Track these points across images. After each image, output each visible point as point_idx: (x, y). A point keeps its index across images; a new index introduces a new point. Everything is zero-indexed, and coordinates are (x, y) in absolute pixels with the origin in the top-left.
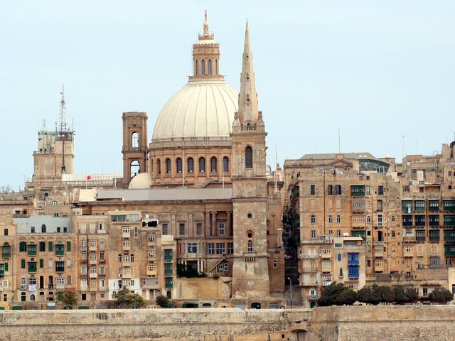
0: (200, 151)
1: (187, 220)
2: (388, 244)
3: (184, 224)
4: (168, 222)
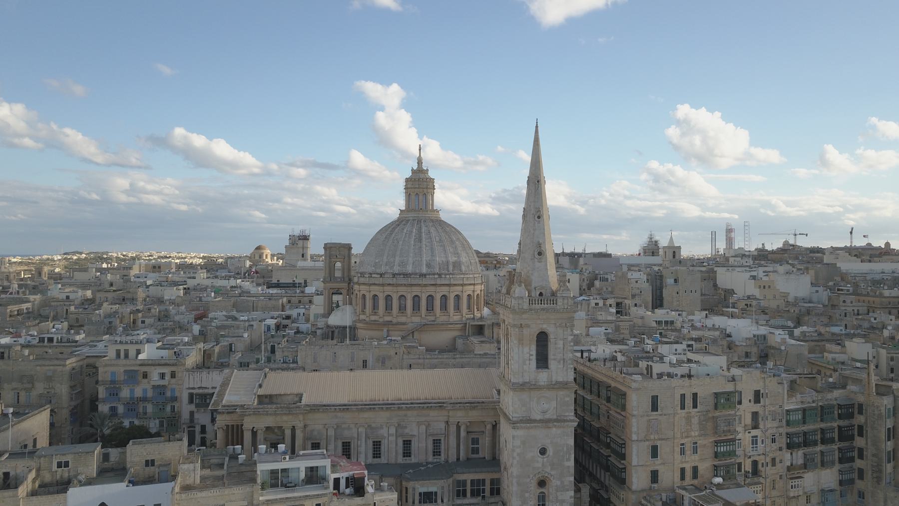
0: (415, 289)
1: (415, 434)
3: (410, 441)
4: (385, 438)
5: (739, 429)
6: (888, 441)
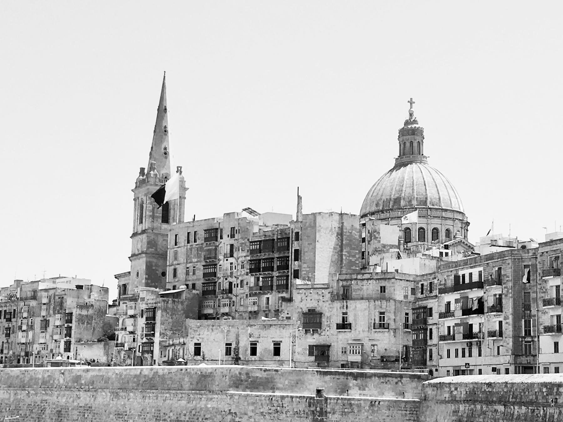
2: (236, 296)
5: (221, 257)
6: (295, 260)
